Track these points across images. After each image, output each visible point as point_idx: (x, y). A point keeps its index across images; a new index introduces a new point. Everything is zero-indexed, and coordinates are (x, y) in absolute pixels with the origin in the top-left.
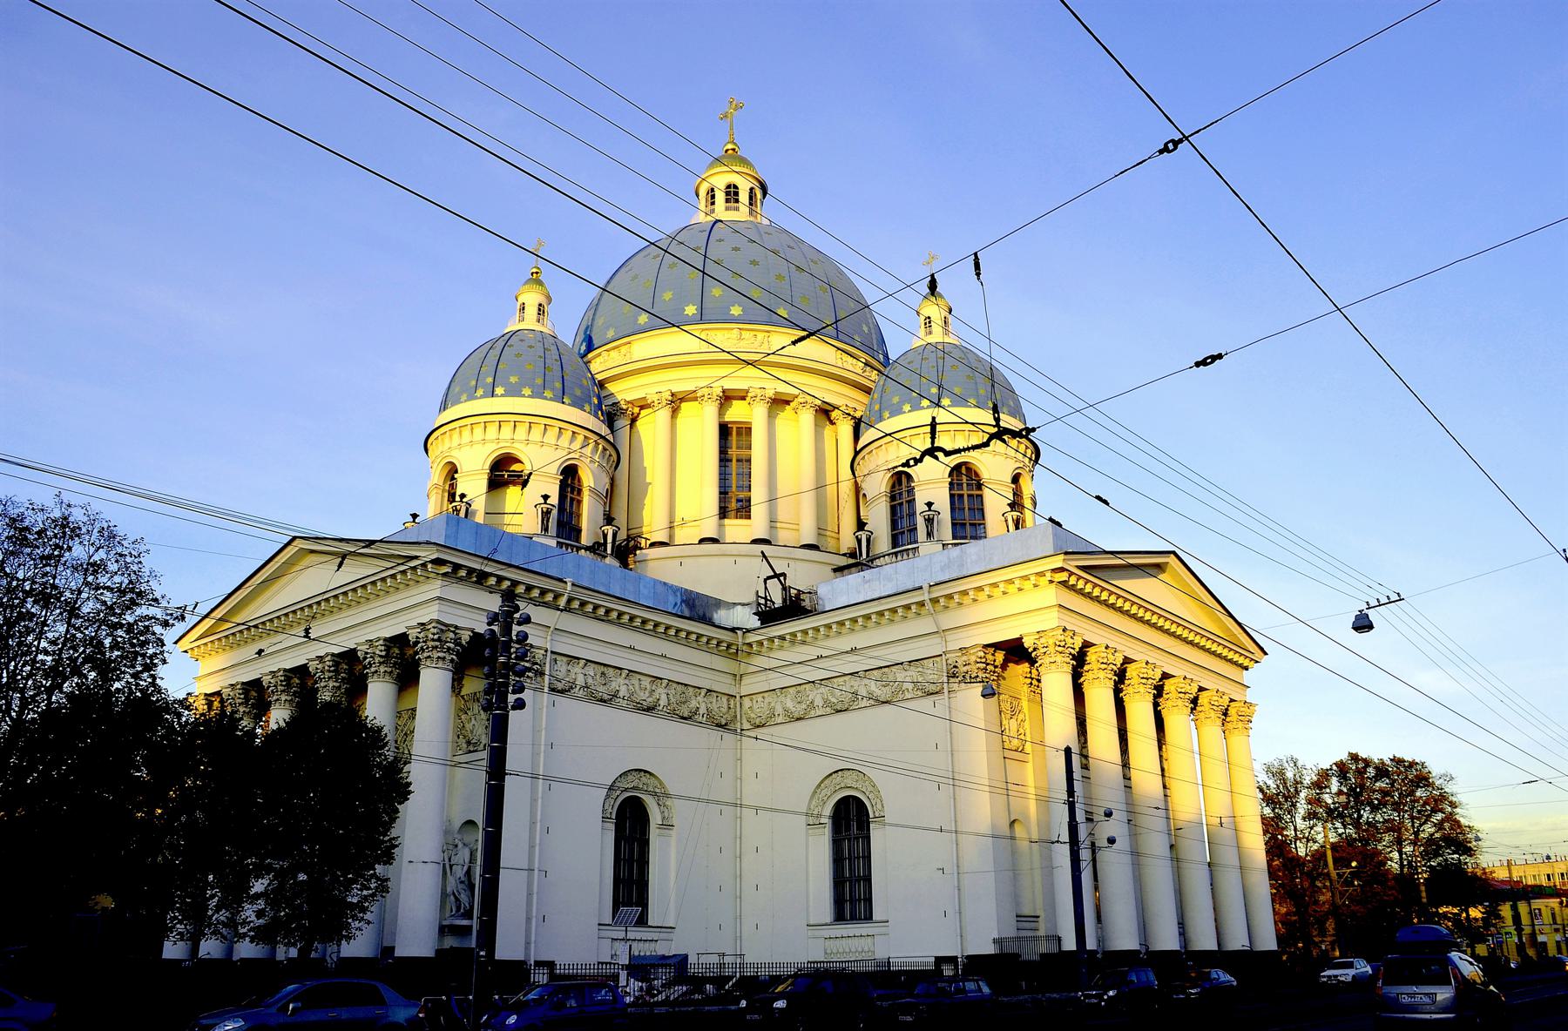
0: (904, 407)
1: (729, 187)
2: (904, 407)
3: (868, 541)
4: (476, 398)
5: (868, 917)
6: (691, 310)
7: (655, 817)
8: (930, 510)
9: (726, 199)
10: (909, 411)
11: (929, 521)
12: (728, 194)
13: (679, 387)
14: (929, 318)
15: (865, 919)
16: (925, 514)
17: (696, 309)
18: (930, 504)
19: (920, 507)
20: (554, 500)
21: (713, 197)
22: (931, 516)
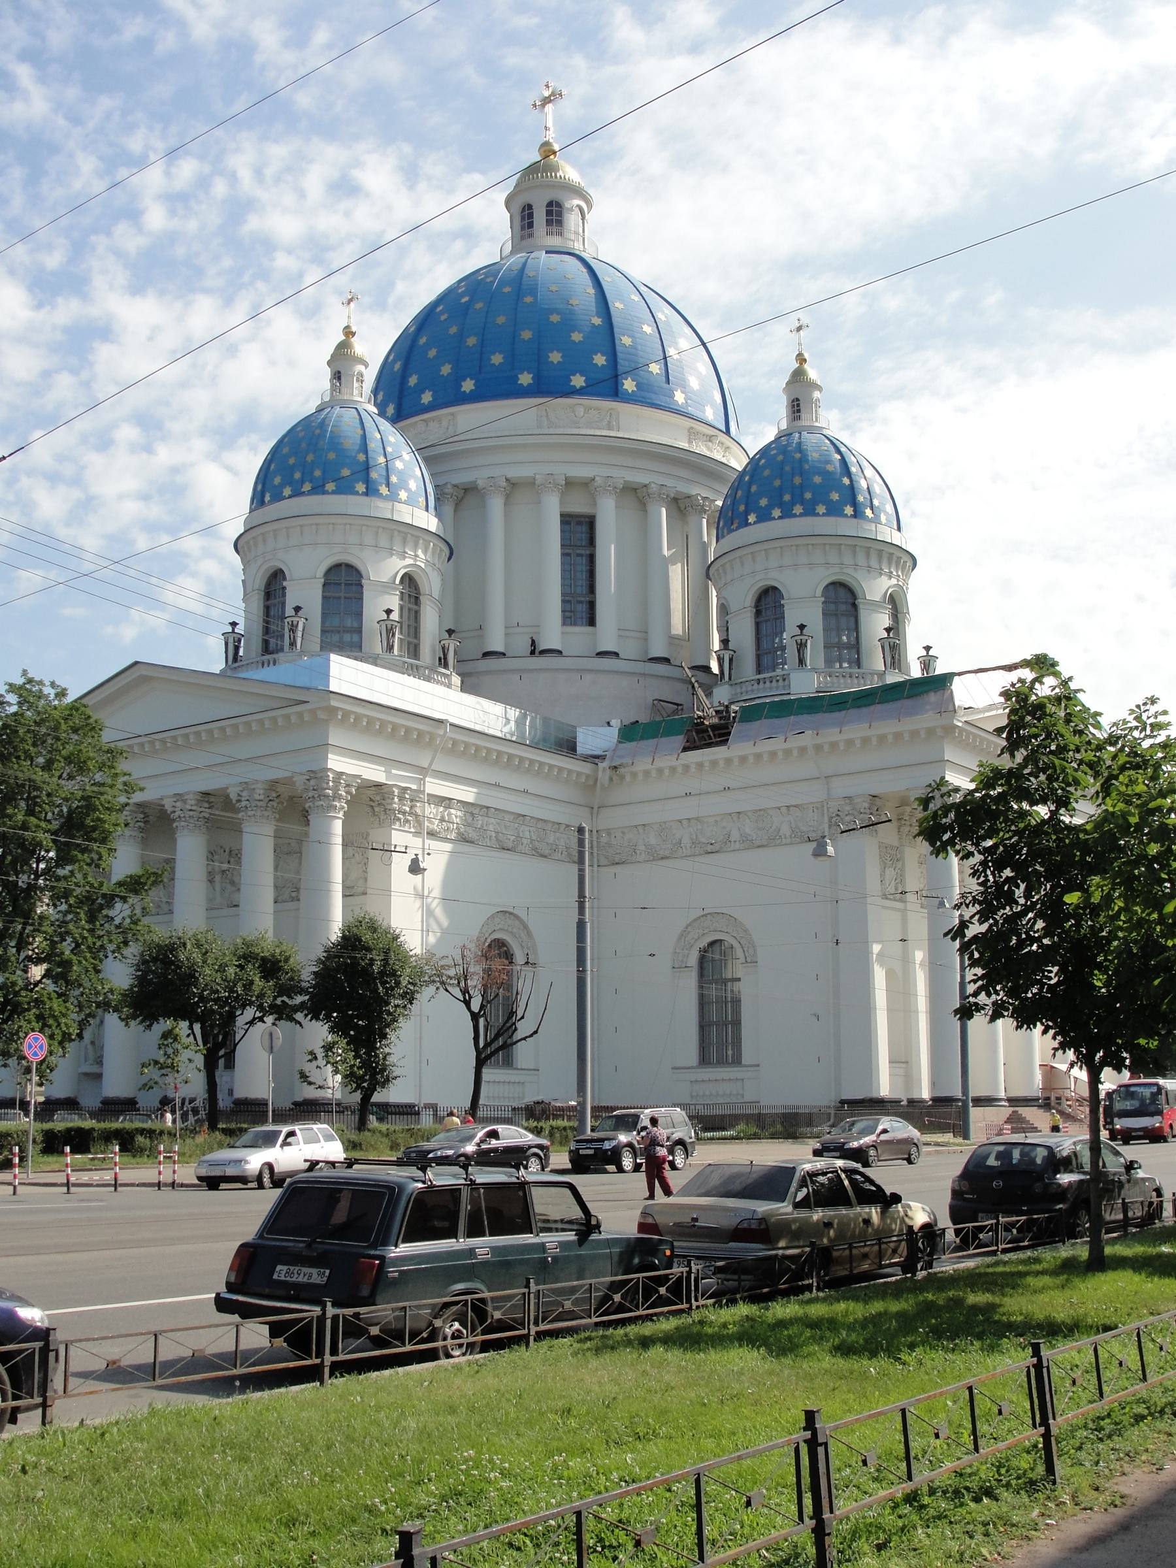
0: (773, 512)
1: (550, 204)
2: (773, 512)
3: (731, 660)
4: (303, 494)
5: (737, 1061)
6: (525, 379)
7: (520, 958)
8: (802, 634)
9: (547, 220)
10: (780, 518)
11: (801, 646)
12: (549, 213)
13: (515, 473)
14: (798, 400)
15: (733, 1062)
16: (796, 638)
17: (533, 378)
18: (802, 627)
19: (790, 629)
20: (395, 616)
21: (531, 215)
22: (804, 641)
